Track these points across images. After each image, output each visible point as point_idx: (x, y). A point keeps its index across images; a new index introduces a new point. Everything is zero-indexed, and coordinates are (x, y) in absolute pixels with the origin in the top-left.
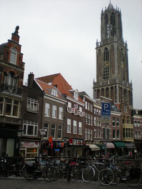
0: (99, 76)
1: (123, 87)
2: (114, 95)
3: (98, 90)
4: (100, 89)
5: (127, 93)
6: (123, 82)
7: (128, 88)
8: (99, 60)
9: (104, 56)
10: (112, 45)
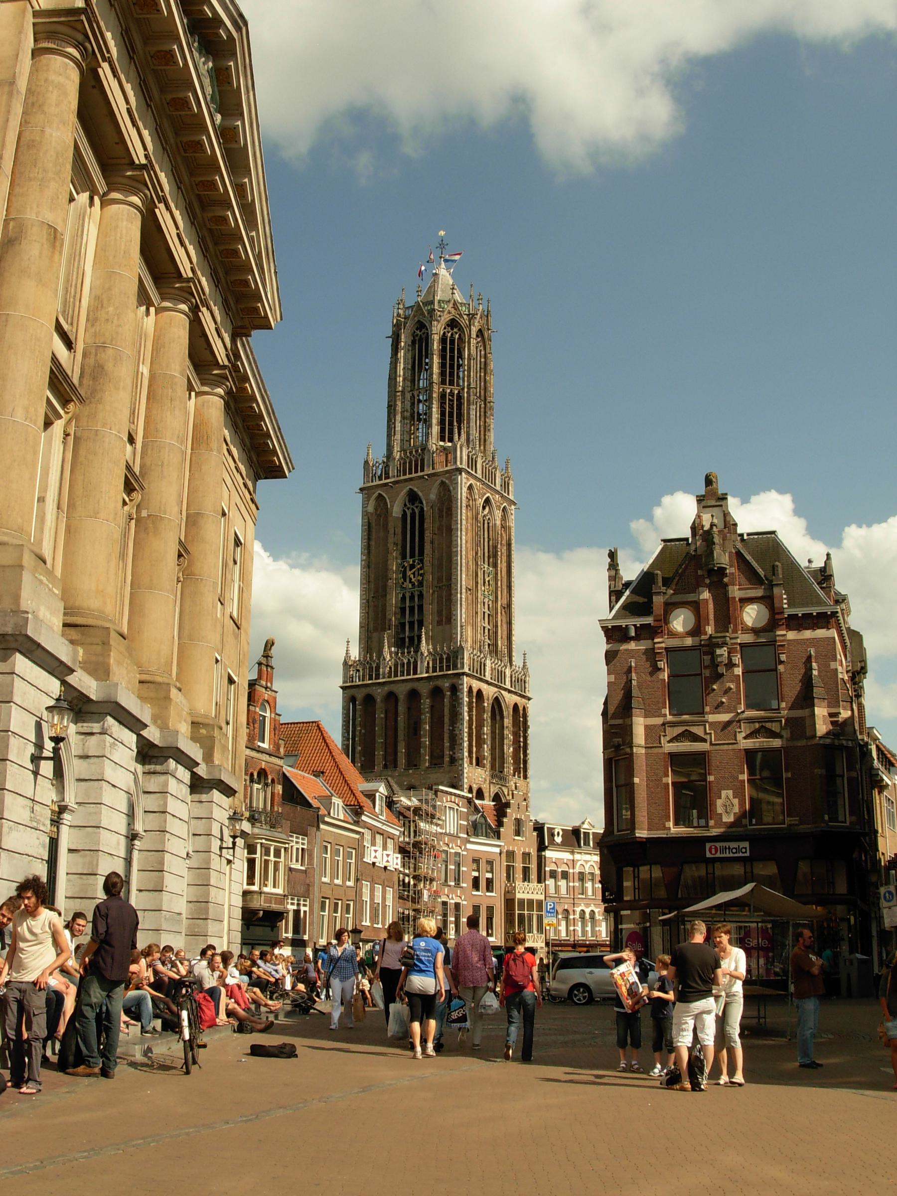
0: (376, 629)
1: (489, 692)
2: (446, 727)
3: (369, 700)
4: (379, 694)
5: (502, 717)
6: (488, 669)
7: (510, 692)
8: (373, 548)
9: (399, 530)
10: (443, 483)
